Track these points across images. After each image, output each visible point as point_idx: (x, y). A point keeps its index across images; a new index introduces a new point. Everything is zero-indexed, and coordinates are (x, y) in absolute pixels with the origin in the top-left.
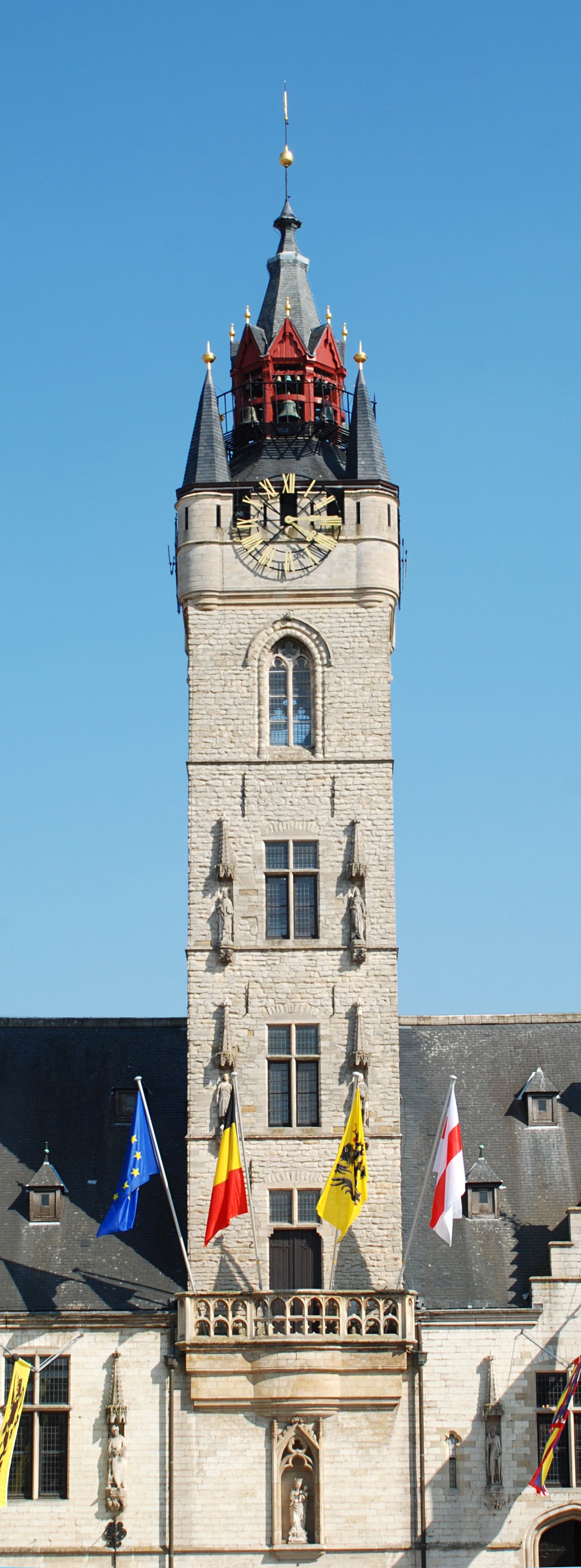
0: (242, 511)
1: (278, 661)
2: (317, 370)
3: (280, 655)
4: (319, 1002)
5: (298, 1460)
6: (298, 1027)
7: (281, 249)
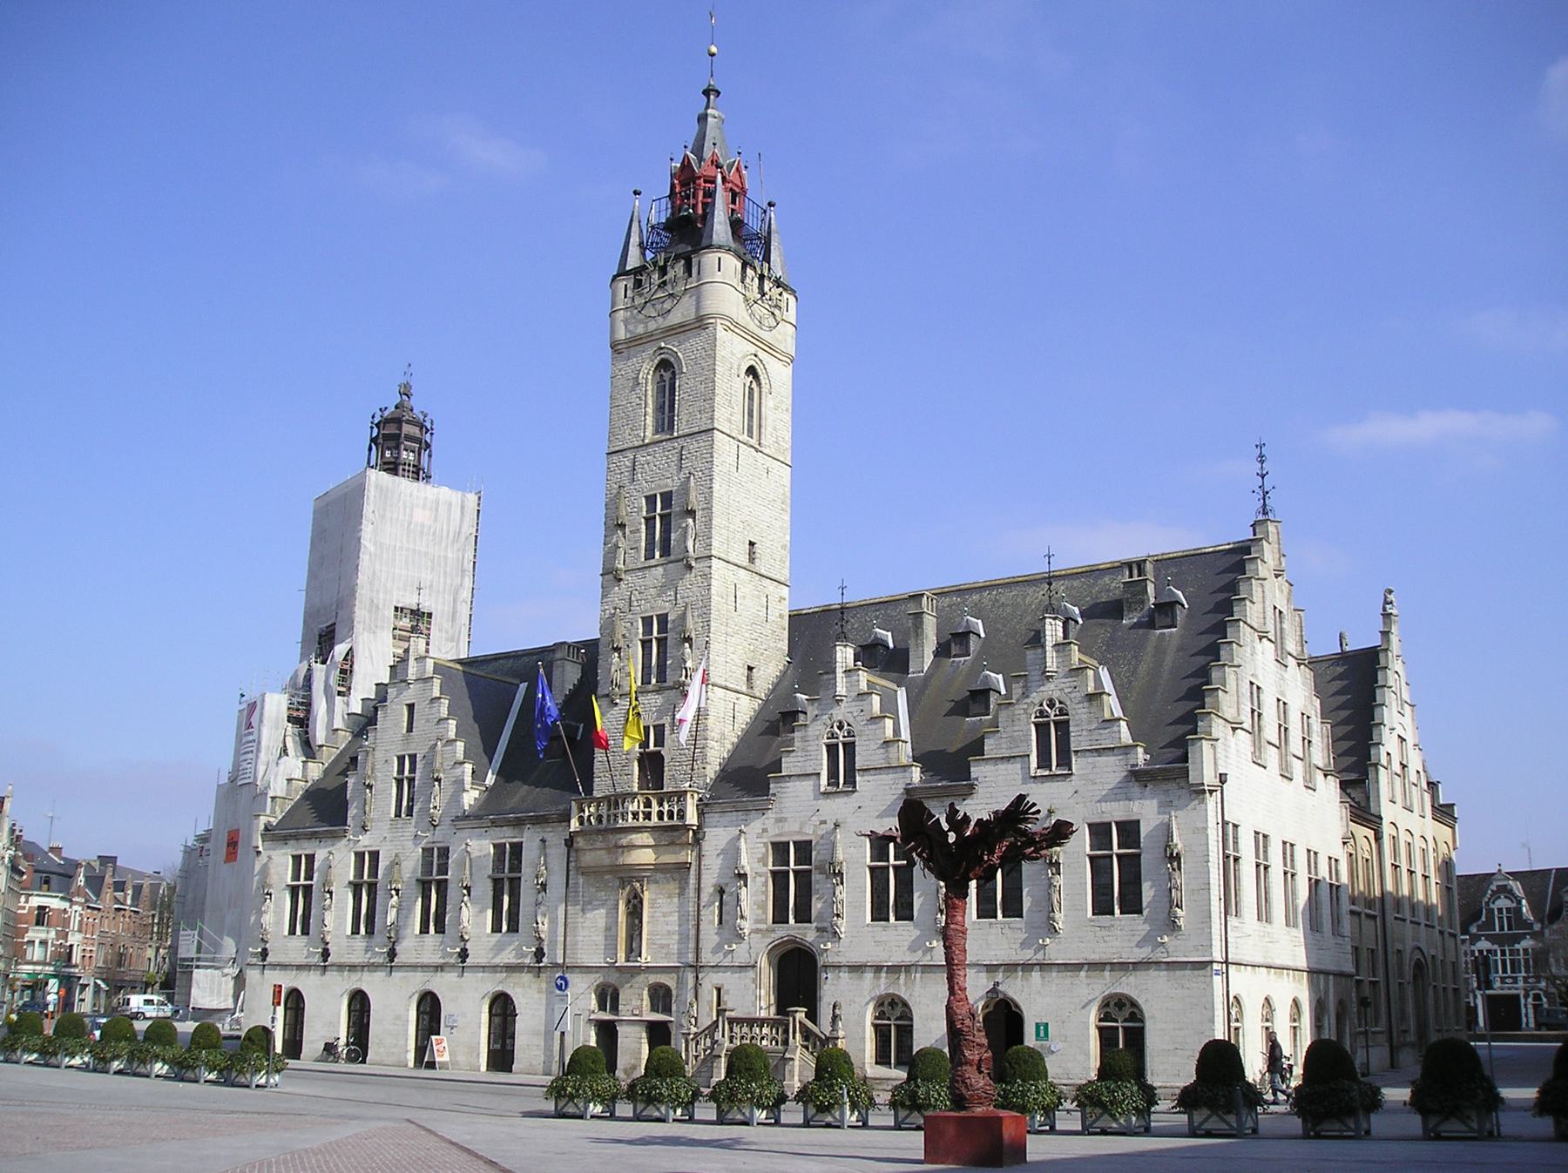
0: (638, 284)
1: (661, 375)
2: (705, 182)
3: (662, 372)
4: (669, 598)
5: (634, 906)
6: (657, 616)
7: (707, 107)
